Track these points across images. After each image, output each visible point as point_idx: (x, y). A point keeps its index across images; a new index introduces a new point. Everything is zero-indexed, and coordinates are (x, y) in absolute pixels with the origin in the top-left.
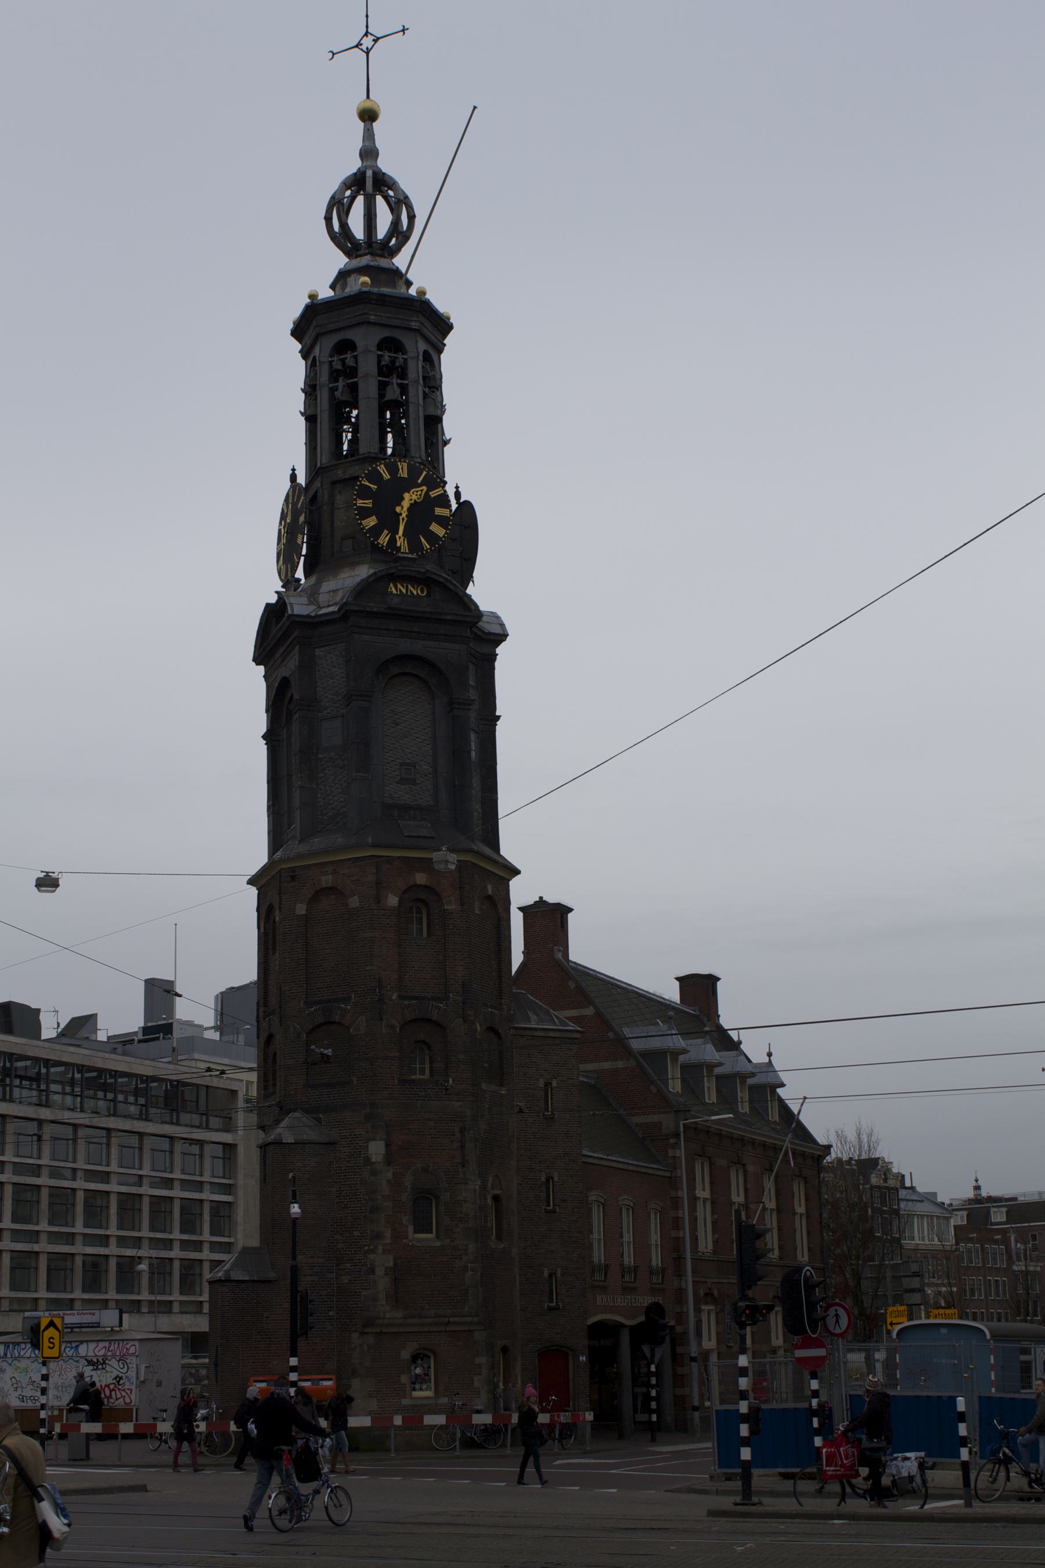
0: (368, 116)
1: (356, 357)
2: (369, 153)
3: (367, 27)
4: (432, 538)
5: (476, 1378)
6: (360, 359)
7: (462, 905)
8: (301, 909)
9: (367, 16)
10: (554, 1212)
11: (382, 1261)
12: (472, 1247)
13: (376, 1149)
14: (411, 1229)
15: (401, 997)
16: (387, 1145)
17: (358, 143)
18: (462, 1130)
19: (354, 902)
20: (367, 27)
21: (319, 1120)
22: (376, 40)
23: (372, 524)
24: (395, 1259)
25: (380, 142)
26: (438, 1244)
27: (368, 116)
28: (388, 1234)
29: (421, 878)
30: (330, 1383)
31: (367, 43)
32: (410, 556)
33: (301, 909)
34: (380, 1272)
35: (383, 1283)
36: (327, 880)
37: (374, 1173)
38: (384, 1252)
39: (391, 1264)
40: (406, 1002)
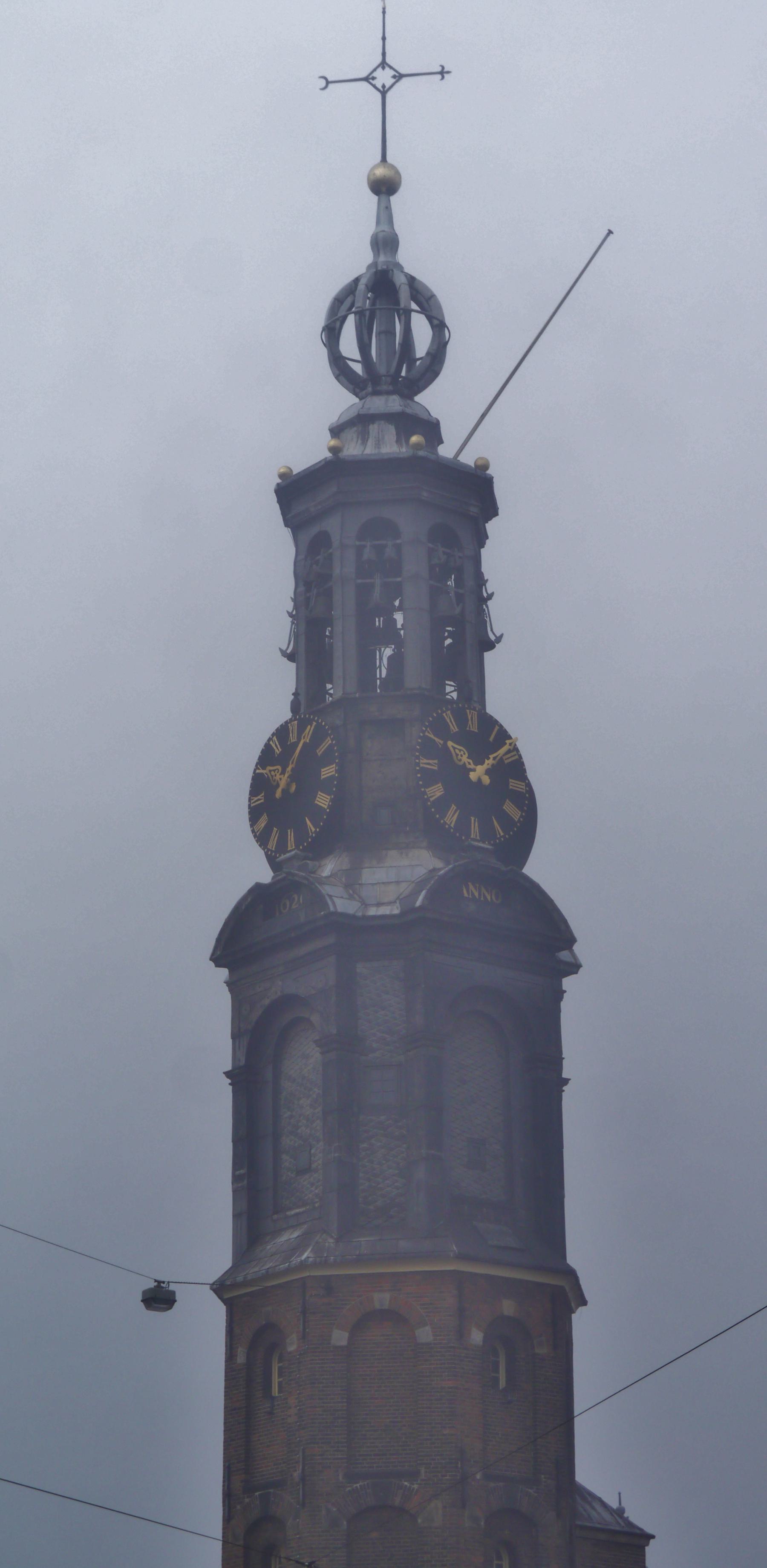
0: (385, 187)
2: (385, 242)
3: (384, 54)
4: (505, 819)
8: (340, 1338)
9: (384, 39)
17: (368, 227)
19: (425, 1334)
20: (384, 54)
22: (399, 77)
23: (438, 794)
25: (400, 227)
27: (385, 187)
29: (508, 1307)
31: (384, 79)
32: (481, 845)
33: (340, 1338)
36: (382, 1299)
40: (492, 1485)
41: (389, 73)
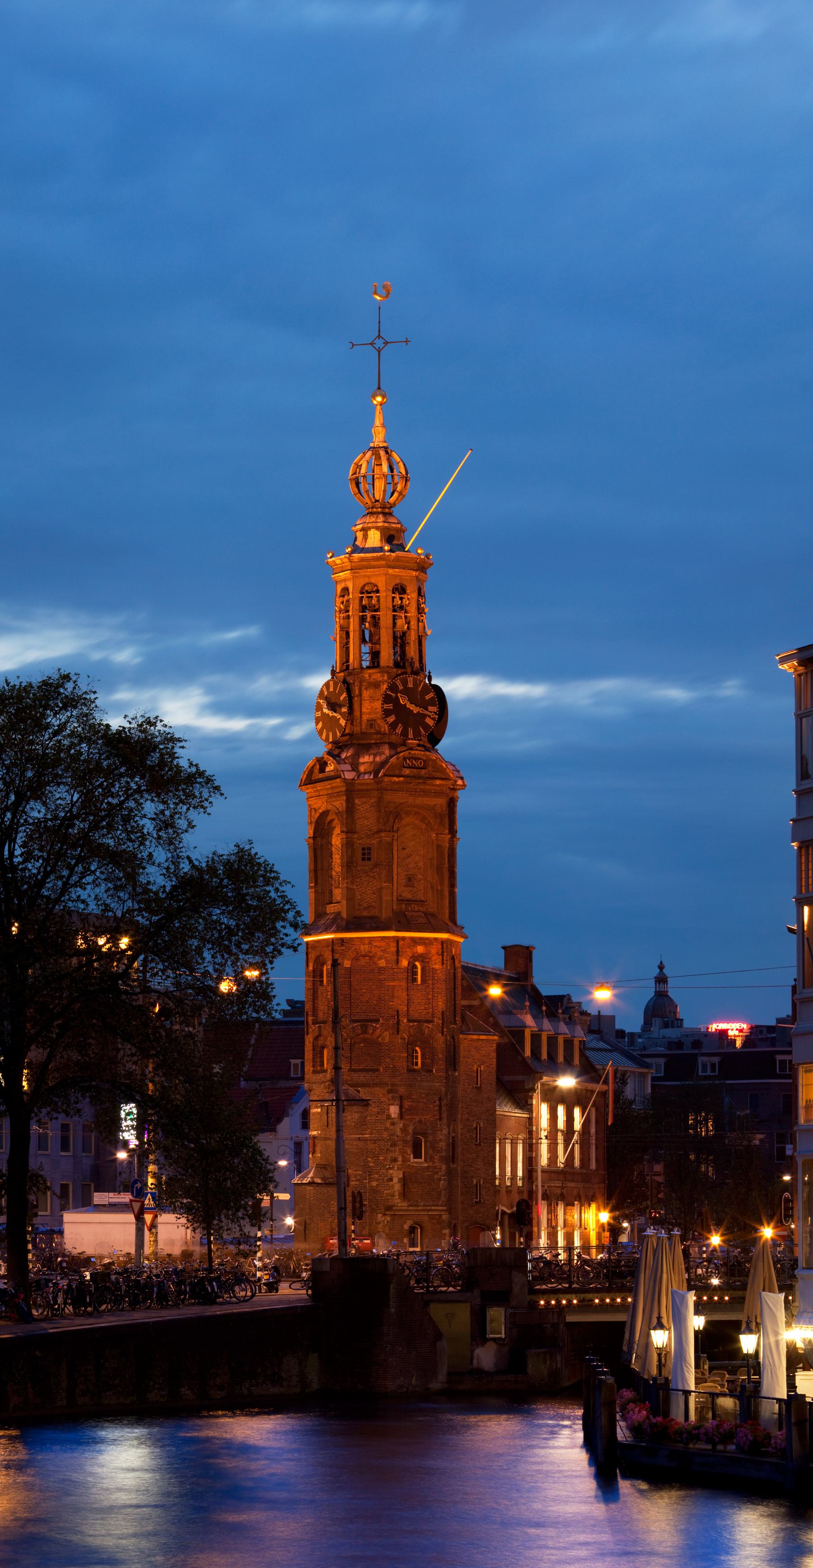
1: (378, 597)
4: (426, 727)
5: (443, 1241)
6: (381, 600)
7: (443, 964)
10: (480, 1144)
11: (397, 1175)
12: (444, 1167)
13: (394, 1110)
14: (412, 1156)
15: (409, 1021)
16: (401, 1108)
18: (440, 1099)
19: (382, 963)
21: (359, 1091)
22: (386, 343)
23: (392, 720)
24: (404, 1173)
26: (426, 1165)
28: (400, 1159)
29: (420, 949)
30: (369, 1241)
34: (395, 1180)
35: (397, 1187)
37: (393, 1124)
38: (398, 1169)
39: (401, 1176)
41: (382, 341)
